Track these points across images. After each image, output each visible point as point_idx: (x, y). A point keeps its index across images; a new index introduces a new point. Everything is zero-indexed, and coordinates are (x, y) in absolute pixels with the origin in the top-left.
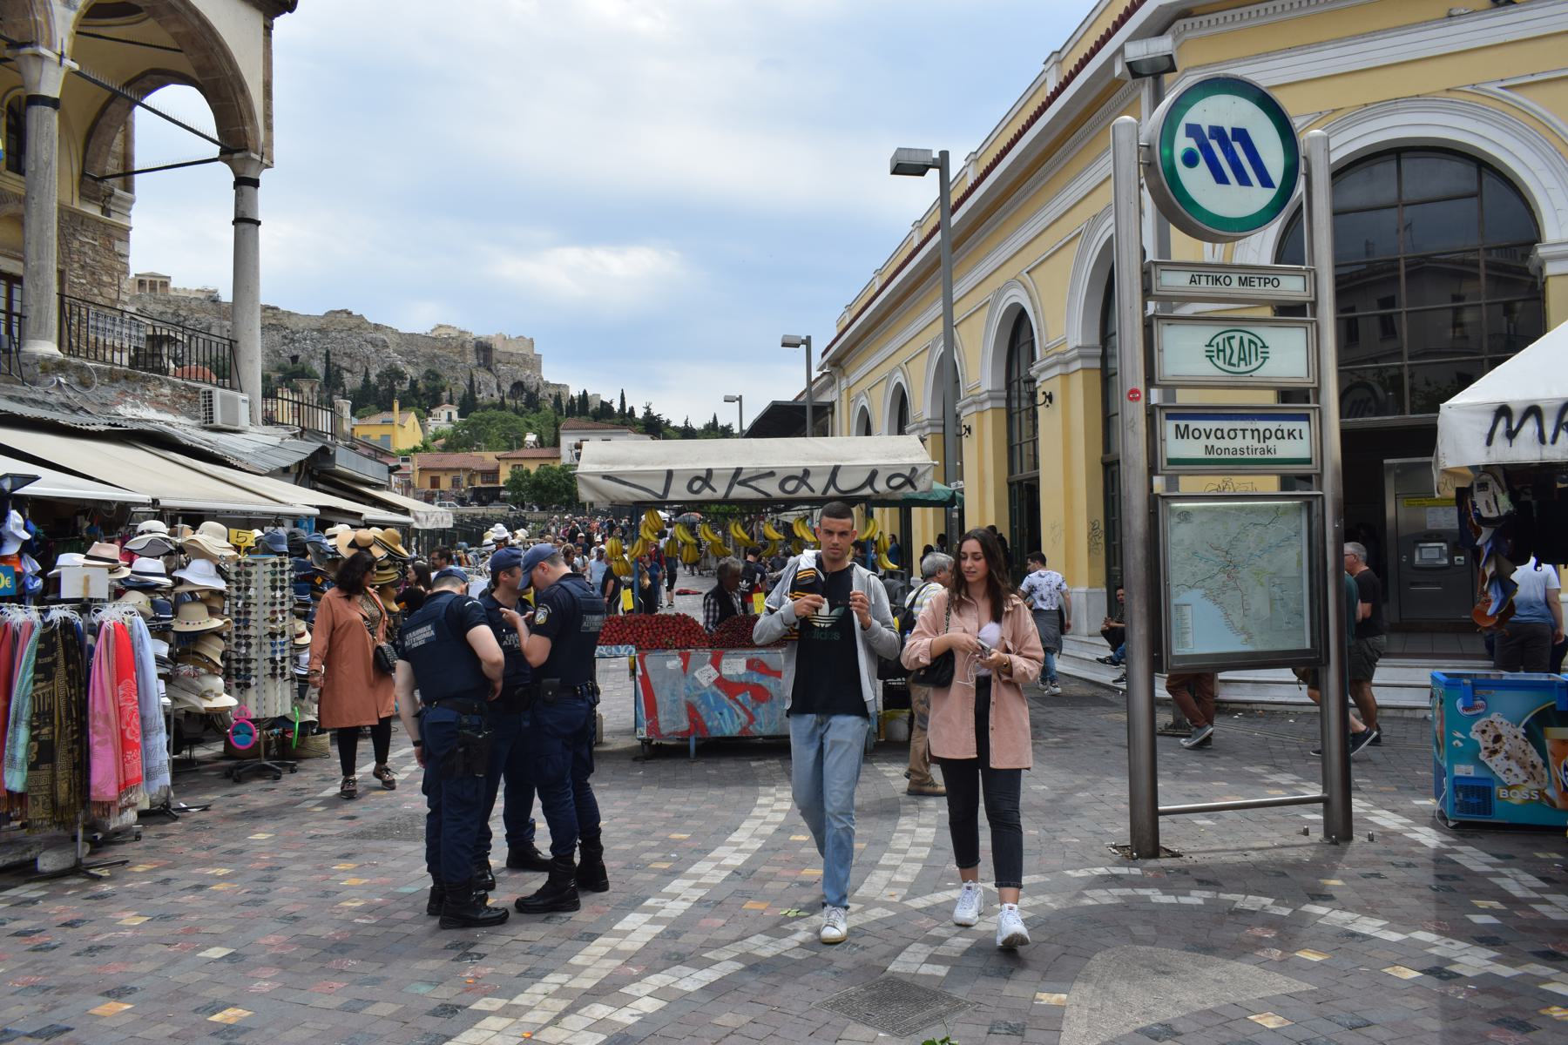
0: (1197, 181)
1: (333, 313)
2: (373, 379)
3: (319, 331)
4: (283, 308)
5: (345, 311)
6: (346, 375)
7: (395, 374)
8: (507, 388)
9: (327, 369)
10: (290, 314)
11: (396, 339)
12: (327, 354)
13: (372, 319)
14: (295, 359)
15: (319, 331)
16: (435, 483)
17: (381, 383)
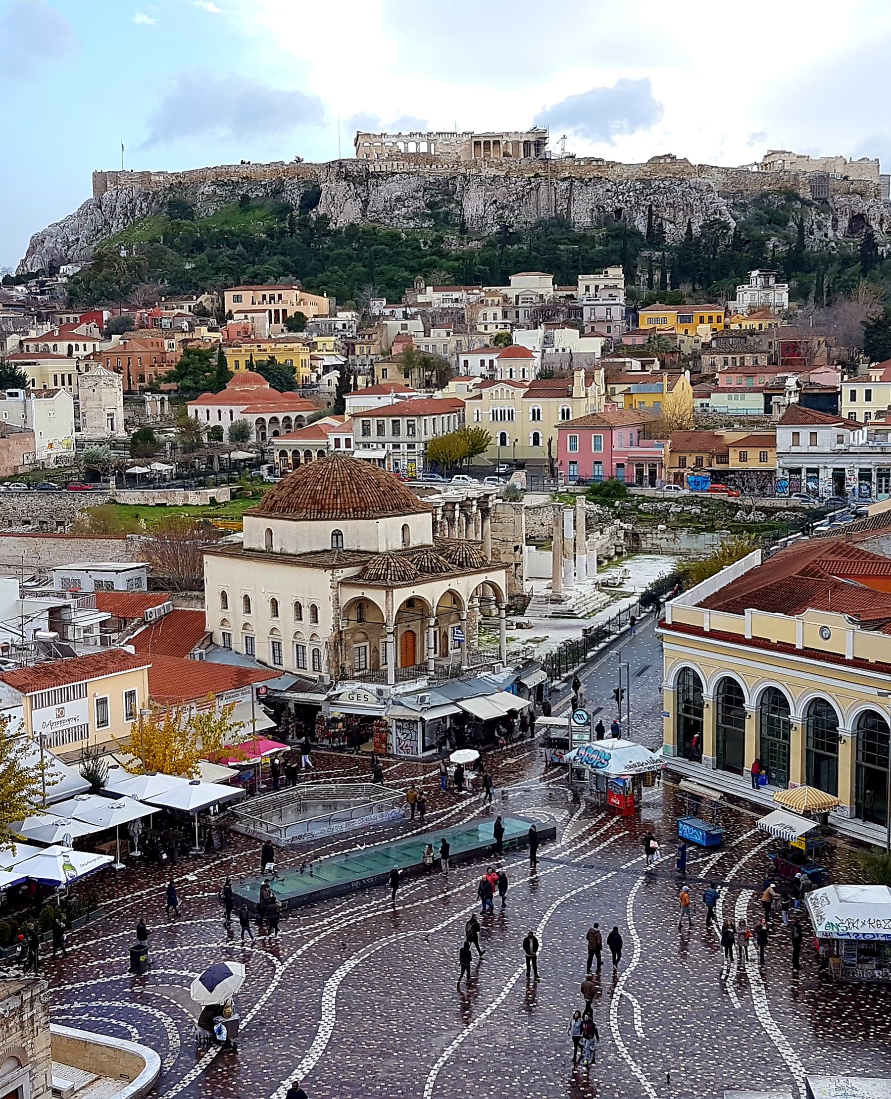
0: (577, 720)
1: (655, 161)
2: (696, 228)
3: (641, 180)
4: (607, 159)
5: (669, 156)
6: (668, 227)
7: (714, 226)
8: (844, 223)
9: (650, 223)
10: (613, 164)
11: (721, 178)
12: (650, 210)
13: (695, 161)
14: (619, 211)
15: (641, 180)
16: (683, 463)
17: (703, 235)
